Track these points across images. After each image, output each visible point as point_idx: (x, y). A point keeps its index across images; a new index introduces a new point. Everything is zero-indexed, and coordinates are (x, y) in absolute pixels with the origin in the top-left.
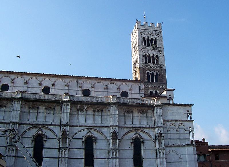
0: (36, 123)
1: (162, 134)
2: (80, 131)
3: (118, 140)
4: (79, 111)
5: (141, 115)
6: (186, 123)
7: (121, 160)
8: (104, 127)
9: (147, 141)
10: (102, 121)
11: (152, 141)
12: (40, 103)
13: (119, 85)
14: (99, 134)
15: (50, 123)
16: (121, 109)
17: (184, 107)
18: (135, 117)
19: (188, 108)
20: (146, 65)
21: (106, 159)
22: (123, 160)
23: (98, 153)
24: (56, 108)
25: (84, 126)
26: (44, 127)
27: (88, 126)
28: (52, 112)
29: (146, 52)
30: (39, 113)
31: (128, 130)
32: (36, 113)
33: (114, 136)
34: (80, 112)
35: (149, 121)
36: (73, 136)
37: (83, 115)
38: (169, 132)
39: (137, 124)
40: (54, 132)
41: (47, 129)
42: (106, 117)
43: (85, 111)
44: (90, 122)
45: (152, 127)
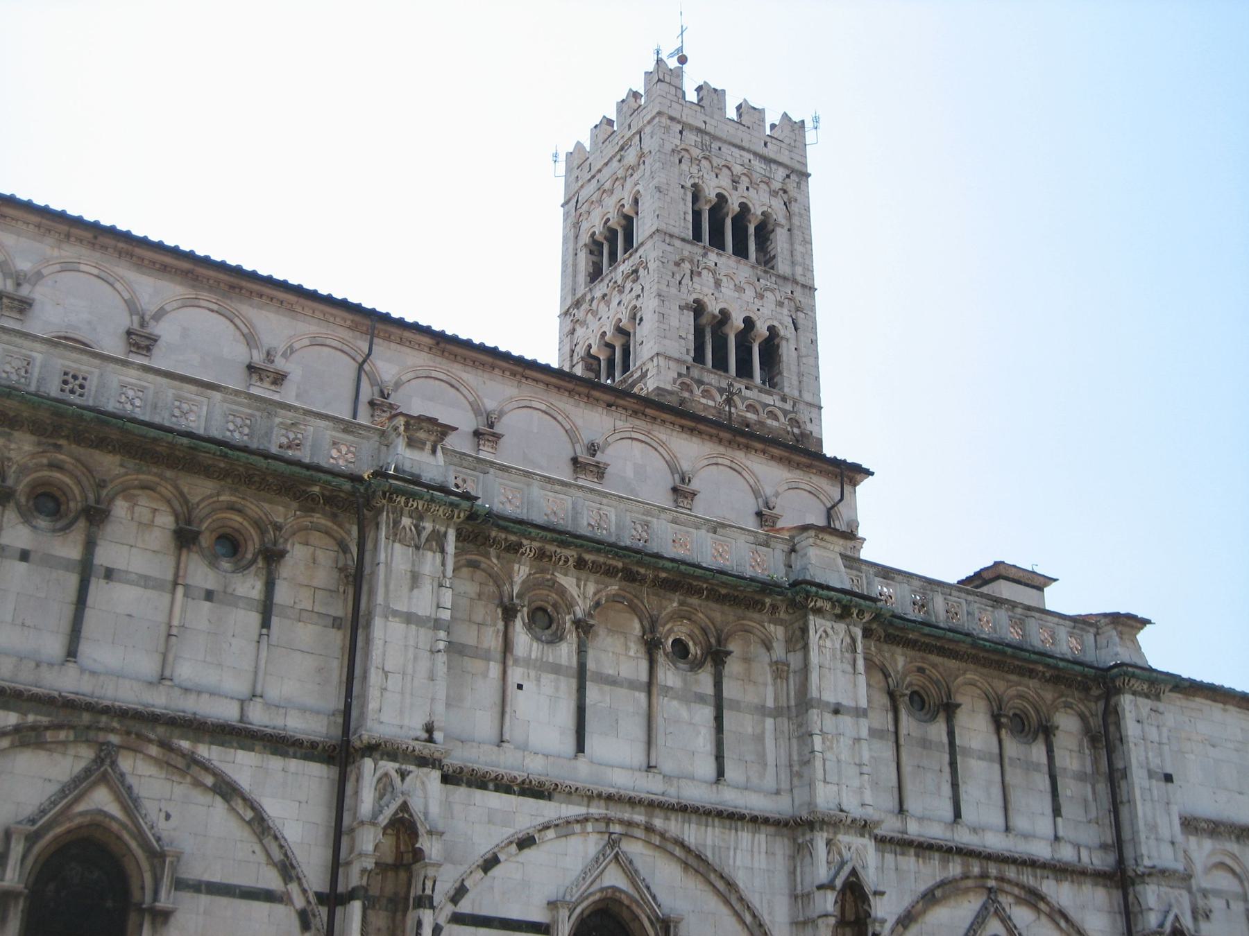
0: (67, 682)
2: (525, 842)
4: (518, 626)
8: (742, 817)
10: (719, 758)
12: (131, 464)
15: (227, 712)
20: (700, 382)
24: (297, 553)
25: (572, 793)
26: (154, 750)
27: (610, 798)
28: (250, 586)
29: (703, 288)
30: (109, 574)
32: (66, 565)
34: (522, 639)
36: (460, 893)
37: (556, 669)
40: (260, 825)
41: (183, 773)
43: (572, 639)
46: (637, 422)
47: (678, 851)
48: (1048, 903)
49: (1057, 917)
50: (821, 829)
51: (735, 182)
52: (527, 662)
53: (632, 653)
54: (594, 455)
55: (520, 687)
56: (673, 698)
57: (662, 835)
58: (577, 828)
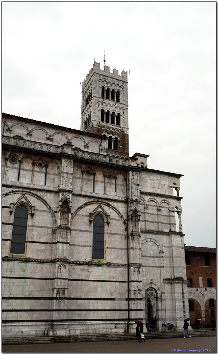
1: (137, 212)
3: (70, 214)
4: (8, 162)
5: (107, 180)
6: (171, 201)
7: (72, 247)
9: (114, 221)
10: (45, 182)
11: (122, 222)
13: (70, 138)
14: (39, 202)
16: (78, 167)
17: (170, 178)
18: (99, 183)
19: (174, 180)
21: (47, 243)
22: (76, 247)
23: (35, 233)
31: (87, 200)
33: (65, 206)
35: (118, 191)
37: (15, 168)
38: (147, 211)
39: (99, 191)
42: (52, 177)
44: (25, 181)
45: (123, 200)
46: (60, 131)
47: (36, 196)
48: (111, 206)
49: (113, 208)
50: (61, 192)
51: (111, 85)
52: (10, 167)
53: (30, 165)
54: (50, 137)
55: (8, 171)
56: (37, 172)
57: (33, 194)
58: (17, 192)
